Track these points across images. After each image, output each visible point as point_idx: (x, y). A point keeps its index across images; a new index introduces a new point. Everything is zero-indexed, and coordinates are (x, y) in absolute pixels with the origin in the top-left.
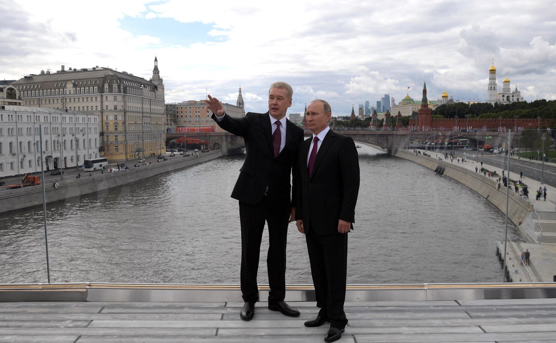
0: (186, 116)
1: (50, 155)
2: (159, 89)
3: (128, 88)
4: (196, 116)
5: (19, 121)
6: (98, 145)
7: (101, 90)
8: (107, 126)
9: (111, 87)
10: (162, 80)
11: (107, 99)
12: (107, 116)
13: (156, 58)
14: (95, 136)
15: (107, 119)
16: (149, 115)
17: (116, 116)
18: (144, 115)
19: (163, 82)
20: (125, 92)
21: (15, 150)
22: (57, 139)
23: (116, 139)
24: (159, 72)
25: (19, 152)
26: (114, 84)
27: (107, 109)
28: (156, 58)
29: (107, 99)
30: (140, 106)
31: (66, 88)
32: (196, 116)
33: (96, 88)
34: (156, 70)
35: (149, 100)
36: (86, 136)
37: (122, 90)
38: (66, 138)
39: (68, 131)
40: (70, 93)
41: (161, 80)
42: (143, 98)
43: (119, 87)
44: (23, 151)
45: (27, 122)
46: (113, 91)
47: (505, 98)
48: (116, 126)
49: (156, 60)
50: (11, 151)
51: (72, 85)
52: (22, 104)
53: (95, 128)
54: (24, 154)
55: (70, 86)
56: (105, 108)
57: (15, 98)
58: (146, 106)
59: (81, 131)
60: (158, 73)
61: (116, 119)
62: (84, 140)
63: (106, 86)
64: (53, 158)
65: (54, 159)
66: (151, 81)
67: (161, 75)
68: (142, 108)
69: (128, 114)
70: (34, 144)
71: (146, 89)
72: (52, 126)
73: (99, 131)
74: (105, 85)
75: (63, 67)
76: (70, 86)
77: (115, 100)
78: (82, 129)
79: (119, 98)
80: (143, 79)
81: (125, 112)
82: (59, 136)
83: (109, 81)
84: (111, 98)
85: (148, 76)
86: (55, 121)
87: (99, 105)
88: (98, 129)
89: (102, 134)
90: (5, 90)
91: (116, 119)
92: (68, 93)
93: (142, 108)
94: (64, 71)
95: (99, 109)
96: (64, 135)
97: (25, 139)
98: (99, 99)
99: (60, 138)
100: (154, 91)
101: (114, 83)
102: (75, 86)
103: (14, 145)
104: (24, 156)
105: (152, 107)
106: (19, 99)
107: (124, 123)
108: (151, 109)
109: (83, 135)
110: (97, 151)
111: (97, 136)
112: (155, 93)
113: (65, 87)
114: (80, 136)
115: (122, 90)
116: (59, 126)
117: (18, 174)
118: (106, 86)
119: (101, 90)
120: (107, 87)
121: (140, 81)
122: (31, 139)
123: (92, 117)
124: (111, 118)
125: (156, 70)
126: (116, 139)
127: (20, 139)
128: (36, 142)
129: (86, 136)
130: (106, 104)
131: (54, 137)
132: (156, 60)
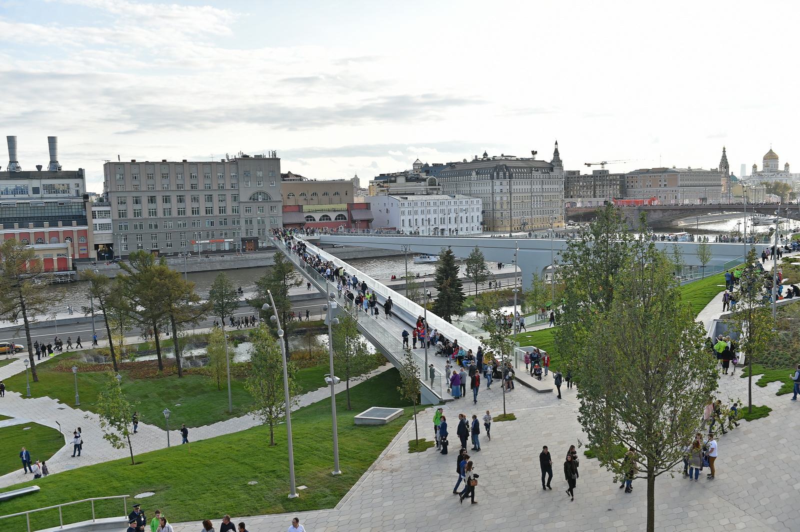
0: (632, 186)
3: (514, 174)
4: (647, 186)
6: (481, 220)
21: (412, 225)
22: (443, 217)
23: (502, 215)
24: (559, 154)
25: (415, 225)
32: (647, 186)
33: (489, 175)
34: (556, 152)
36: (468, 214)
37: (507, 177)
38: (450, 215)
39: (453, 211)
43: (505, 174)
49: (556, 143)
50: (410, 225)
53: (478, 209)
55: (474, 173)
57: (436, 185)
59: (464, 210)
61: (501, 199)
64: (440, 229)
67: (561, 157)
70: (426, 220)
73: (481, 210)
87: (490, 188)
88: (480, 208)
90: (428, 180)
91: (501, 199)
96: (449, 214)
97: (420, 217)
102: (477, 173)
103: (412, 221)
104: (418, 227)
106: (439, 185)
109: (466, 213)
110: (478, 224)
111: (480, 214)
113: (471, 175)
115: (507, 177)
116: (445, 208)
119: (492, 178)
122: (436, 216)
123: (475, 200)
124: (498, 199)
125: (556, 152)
126: (502, 215)
127: (415, 217)
128: (427, 219)
129: (468, 213)
131: (441, 215)
132: (556, 143)
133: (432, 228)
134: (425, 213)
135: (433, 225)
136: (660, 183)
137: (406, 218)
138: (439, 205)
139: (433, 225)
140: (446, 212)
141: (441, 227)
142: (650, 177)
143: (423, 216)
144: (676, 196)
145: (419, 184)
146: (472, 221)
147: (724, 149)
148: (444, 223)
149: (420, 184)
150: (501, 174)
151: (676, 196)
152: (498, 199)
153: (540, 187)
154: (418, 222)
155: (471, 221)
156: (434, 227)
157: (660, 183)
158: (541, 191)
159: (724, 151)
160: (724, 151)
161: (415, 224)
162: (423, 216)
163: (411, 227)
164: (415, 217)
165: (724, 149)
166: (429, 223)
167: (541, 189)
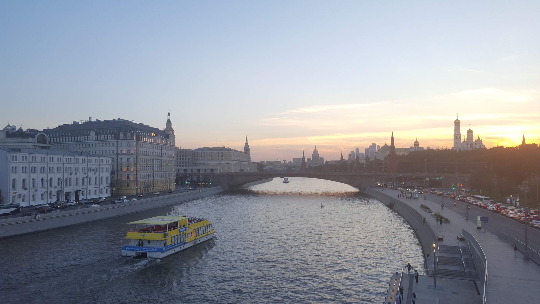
1: (60, 189)
2: (170, 138)
5: (33, 161)
6: (109, 182)
7: (117, 138)
8: (121, 166)
9: (125, 134)
10: (174, 130)
11: (121, 145)
12: (121, 158)
13: (169, 113)
14: (106, 175)
15: (121, 160)
16: (160, 158)
17: (129, 158)
18: (155, 158)
19: (175, 132)
20: (137, 139)
21: (27, 186)
22: (69, 177)
23: (128, 177)
26: (127, 133)
27: (121, 152)
28: (169, 113)
29: (121, 145)
30: (152, 150)
31: (90, 135)
33: (113, 135)
34: (169, 122)
35: (161, 146)
36: (97, 175)
38: (78, 175)
39: (81, 170)
40: (93, 139)
41: (173, 131)
42: (154, 144)
43: (132, 135)
44: (36, 186)
45: (22, 161)
46: (127, 138)
47: (469, 146)
48: (129, 167)
49: (169, 114)
50: (24, 187)
51: (94, 133)
52: (51, 148)
53: (107, 169)
54: (36, 189)
55: (93, 133)
56: (119, 152)
57: (46, 143)
58: (158, 151)
59: (93, 170)
60: (171, 125)
61: (128, 160)
62: (96, 178)
63: (121, 134)
64: (64, 192)
65: (65, 193)
66: (164, 130)
67: (173, 127)
68: (153, 152)
69: (140, 157)
70: (47, 181)
71: (157, 137)
72: (65, 166)
73: (110, 171)
74: (121, 133)
75: (90, 118)
76: (93, 133)
77: (129, 145)
78: (94, 168)
79: (133, 143)
80: (158, 129)
81: (137, 156)
82: (71, 174)
83: (124, 130)
84: (125, 143)
85: (162, 127)
86: (69, 162)
87: (115, 148)
88: (110, 168)
89: (113, 173)
91: (128, 160)
92: (91, 140)
93: (153, 152)
94: (91, 122)
95: (115, 152)
96: (76, 174)
98: (115, 144)
99: (72, 176)
100: (165, 139)
101: (128, 132)
102: (97, 134)
103: (27, 181)
105: (163, 151)
106: (50, 143)
107: (136, 164)
108: (162, 153)
109: (95, 174)
111: (109, 175)
112: (166, 140)
113: (89, 134)
114: (90, 175)
116: (72, 166)
117: (29, 205)
118: (121, 134)
119: (117, 138)
120: (122, 135)
121: (156, 131)
123: (105, 159)
124: (125, 160)
125: (169, 122)
127: (33, 176)
128: (49, 179)
129: (97, 174)
130: (120, 148)
131: (66, 175)
132: (169, 114)
133: (54, 192)
134: (46, 171)
135: (56, 187)
136: (218, 158)
137: (19, 177)
138: (65, 162)
139: (56, 187)
140: (72, 171)
141: (66, 190)
142: (211, 153)
143: (44, 176)
144: (230, 167)
145: (25, 140)
146: (101, 183)
147: (247, 138)
148: (70, 185)
149: (26, 140)
150: (129, 134)
151: (230, 167)
152: (125, 160)
153: (160, 151)
154: (35, 184)
155: (100, 183)
156: (57, 190)
157: (218, 158)
158: (161, 155)
159: (247, 140)
160: (247, 140)
161: (31, 185)
162: (44, 176)
163: (26, 189)
164: (33, 176)
165: (247, 138)
166: (51, 186)
167: (161, 153)
